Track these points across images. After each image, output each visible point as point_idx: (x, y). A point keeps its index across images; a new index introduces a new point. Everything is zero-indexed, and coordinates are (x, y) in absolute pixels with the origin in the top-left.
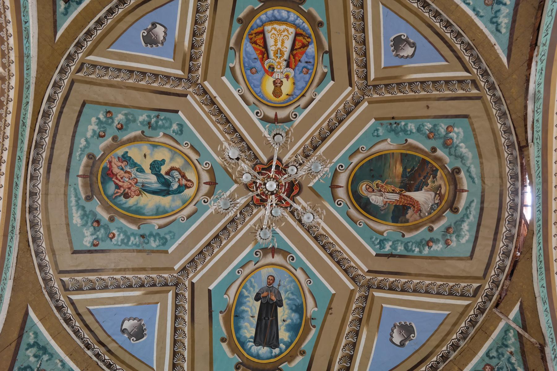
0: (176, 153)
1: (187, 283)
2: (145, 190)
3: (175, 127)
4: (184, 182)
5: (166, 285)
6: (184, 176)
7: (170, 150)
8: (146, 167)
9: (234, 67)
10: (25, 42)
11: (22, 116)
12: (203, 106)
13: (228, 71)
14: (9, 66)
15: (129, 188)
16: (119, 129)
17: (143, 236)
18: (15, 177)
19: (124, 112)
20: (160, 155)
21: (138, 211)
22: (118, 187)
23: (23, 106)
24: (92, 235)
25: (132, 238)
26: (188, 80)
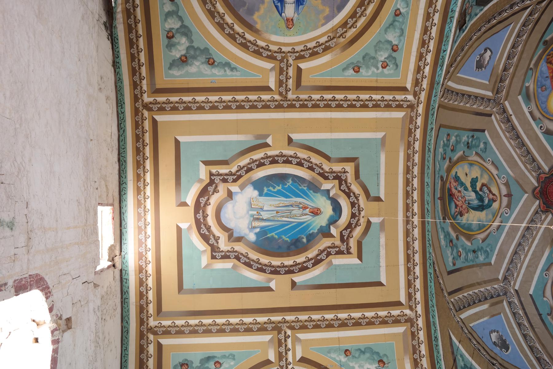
0: (483, 169)
1: (512, 291)
2: (470, 207)
3: (482, 146)
4: (491, 196)
5: (499, 295)
6: (490, 191)
7: (480, 167)
8: (468, 185)
9: (529, 86)
10: (438, 69)
11: (428, 142)
12: (501, 124)
13: (524, 90)
14: (420, 93)
15: (462, 207)
16: (452, 150)
17: (474, 251)
18: (426, 203)
19: (456, 134)
20: (475, 172)
21: (469, 227)
22: (456, 206)
23: (428, 132)
24: (451, 254)
25: (469, 255)
26: (494, 100)
